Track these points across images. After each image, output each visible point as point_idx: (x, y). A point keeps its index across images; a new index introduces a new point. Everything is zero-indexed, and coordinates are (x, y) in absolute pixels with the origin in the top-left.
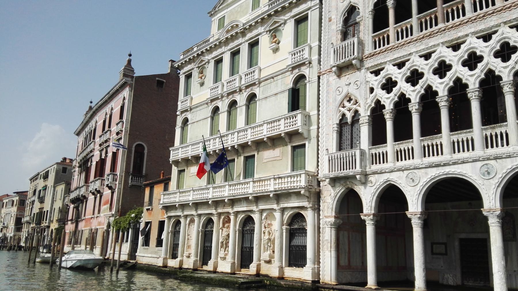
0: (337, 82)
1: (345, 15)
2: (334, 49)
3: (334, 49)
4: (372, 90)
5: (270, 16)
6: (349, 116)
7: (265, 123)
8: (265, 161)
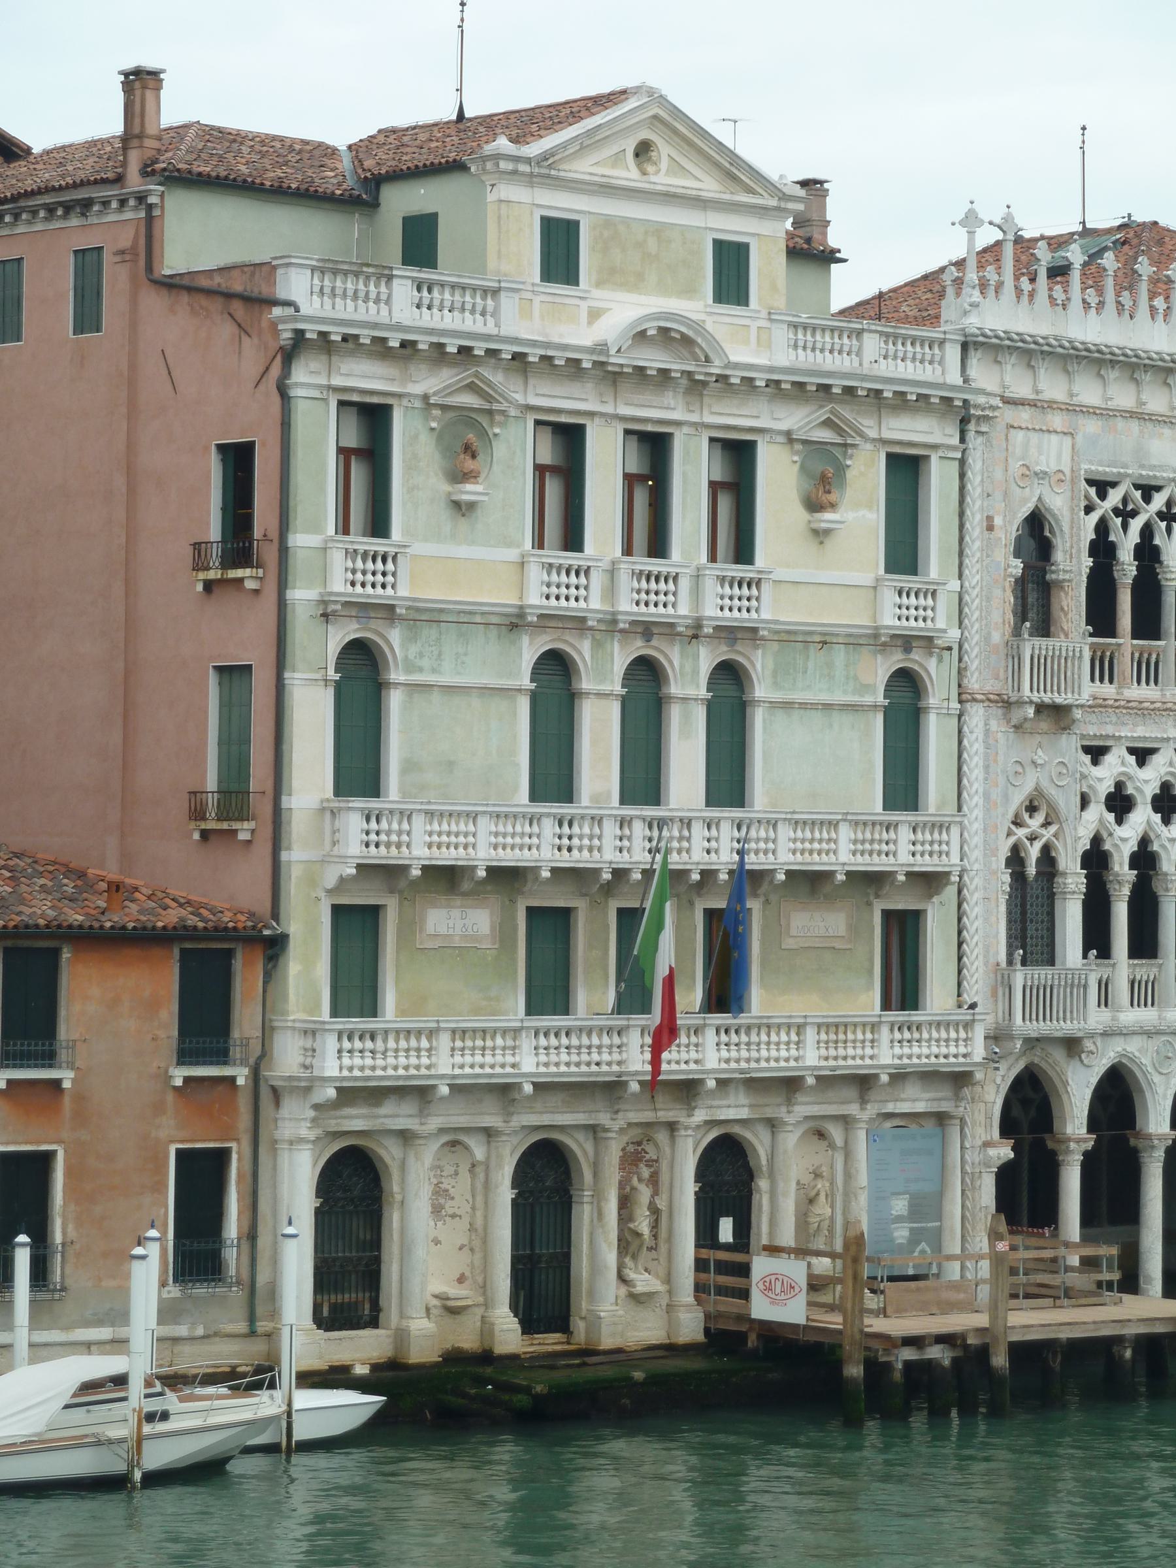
4: (1085, 802)
6: (1033, 852)
7: (845, 820)
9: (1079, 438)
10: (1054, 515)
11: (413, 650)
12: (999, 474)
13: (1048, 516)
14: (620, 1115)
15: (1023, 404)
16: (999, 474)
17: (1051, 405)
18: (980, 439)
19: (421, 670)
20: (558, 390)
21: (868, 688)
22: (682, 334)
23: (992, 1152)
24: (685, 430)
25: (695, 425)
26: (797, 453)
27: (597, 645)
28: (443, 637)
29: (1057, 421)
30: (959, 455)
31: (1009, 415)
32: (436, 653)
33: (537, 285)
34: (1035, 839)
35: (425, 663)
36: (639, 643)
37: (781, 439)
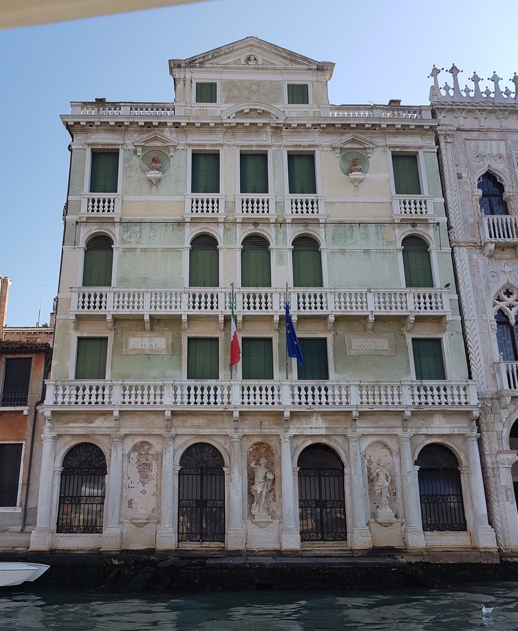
0: (487, 264)
1: (479, 179)
2: (489, 220)
3: (489, 220)
5: (346, 127)
8: (354, 353)
9: (509, 142)
10: (500, 172)
11: (126, 235)
12: (462, 157)
13: (497, 173)
14: (240, 430)
15: (472, 131)
16: (462, 157)
17: (489, 130)
18: (449, 145)
19: (130, 242)
20: (203, 138)
21: (390, 243)
22: (263, 111)
23: (502, 456)
24: (274, 148)
25: (280, 146)
26: (337, 153)
27: (226, 230)
28: (143, 230)
29: (495, 136)
30: (436, 151)
31: (464, 135)
32: (138, 236)
33: (195, 104)
34: (513, 307)
35: (132, 240)
36: (251, 227)
37: (329, 149)
